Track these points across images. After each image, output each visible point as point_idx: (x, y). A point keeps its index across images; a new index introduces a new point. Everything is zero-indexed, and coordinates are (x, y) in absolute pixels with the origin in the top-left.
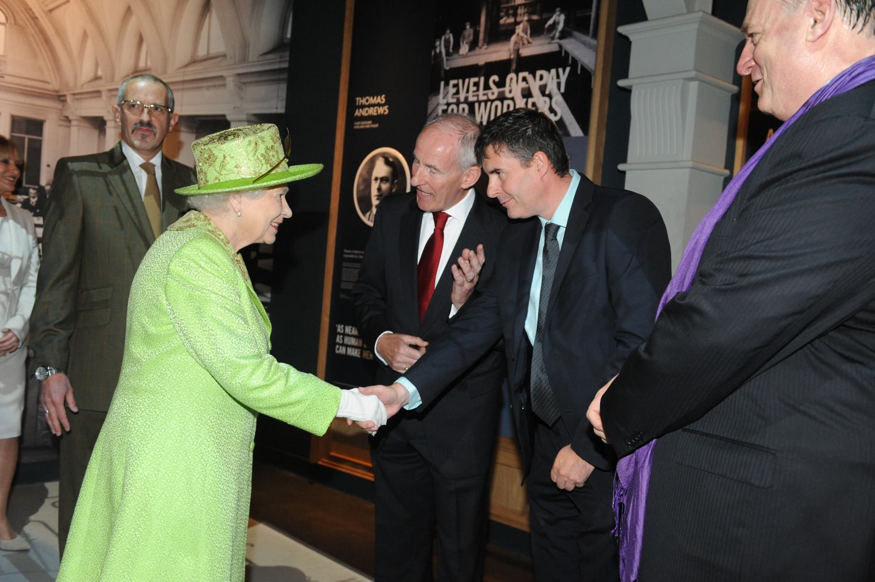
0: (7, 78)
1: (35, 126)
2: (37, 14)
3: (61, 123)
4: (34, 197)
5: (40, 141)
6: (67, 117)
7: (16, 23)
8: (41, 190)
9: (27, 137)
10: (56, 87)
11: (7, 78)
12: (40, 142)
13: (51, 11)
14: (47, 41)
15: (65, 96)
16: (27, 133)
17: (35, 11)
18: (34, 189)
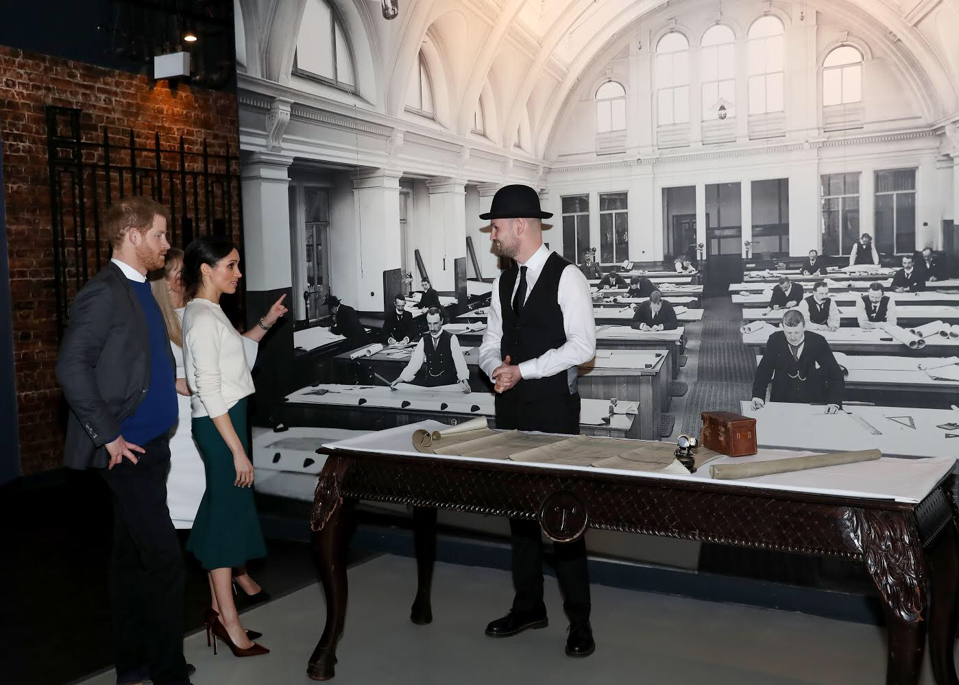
0: (866, 128)
1: (906, 177)
2: (900, 36)
3: (939, 165)
4: (909, 268)
5: (913, 194)
6: (947, 155)
7: (873, 57)
8: (918, 258)
9: (895, 193)
10: (930, 121)
11: (866, 128)
12: (912, 196)
13: (916, 25)
14: (913, 64)
15: (943, 127)
16: (896, 188)
17: (895, 32)
18: (908, 257)
